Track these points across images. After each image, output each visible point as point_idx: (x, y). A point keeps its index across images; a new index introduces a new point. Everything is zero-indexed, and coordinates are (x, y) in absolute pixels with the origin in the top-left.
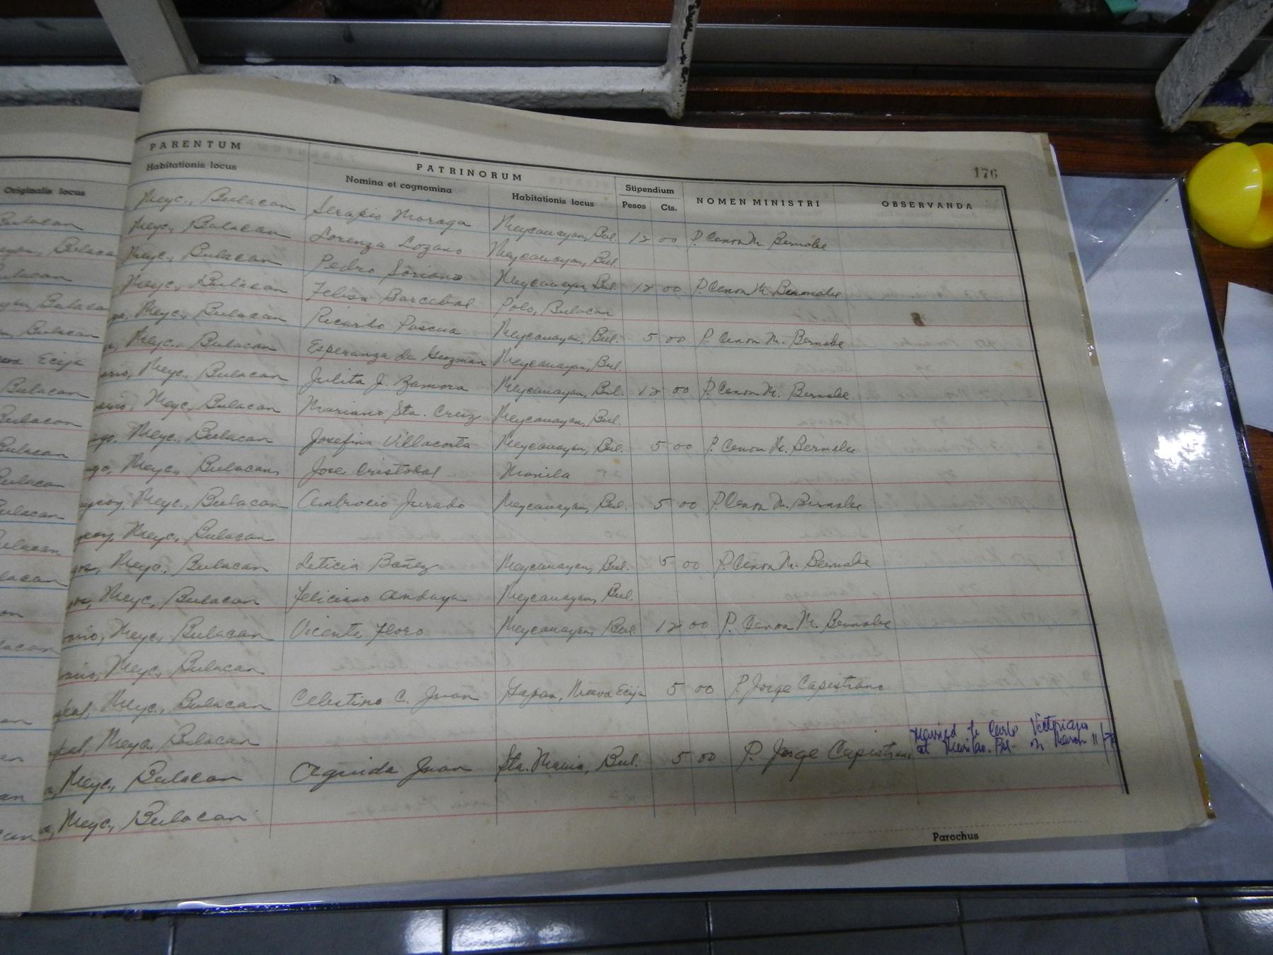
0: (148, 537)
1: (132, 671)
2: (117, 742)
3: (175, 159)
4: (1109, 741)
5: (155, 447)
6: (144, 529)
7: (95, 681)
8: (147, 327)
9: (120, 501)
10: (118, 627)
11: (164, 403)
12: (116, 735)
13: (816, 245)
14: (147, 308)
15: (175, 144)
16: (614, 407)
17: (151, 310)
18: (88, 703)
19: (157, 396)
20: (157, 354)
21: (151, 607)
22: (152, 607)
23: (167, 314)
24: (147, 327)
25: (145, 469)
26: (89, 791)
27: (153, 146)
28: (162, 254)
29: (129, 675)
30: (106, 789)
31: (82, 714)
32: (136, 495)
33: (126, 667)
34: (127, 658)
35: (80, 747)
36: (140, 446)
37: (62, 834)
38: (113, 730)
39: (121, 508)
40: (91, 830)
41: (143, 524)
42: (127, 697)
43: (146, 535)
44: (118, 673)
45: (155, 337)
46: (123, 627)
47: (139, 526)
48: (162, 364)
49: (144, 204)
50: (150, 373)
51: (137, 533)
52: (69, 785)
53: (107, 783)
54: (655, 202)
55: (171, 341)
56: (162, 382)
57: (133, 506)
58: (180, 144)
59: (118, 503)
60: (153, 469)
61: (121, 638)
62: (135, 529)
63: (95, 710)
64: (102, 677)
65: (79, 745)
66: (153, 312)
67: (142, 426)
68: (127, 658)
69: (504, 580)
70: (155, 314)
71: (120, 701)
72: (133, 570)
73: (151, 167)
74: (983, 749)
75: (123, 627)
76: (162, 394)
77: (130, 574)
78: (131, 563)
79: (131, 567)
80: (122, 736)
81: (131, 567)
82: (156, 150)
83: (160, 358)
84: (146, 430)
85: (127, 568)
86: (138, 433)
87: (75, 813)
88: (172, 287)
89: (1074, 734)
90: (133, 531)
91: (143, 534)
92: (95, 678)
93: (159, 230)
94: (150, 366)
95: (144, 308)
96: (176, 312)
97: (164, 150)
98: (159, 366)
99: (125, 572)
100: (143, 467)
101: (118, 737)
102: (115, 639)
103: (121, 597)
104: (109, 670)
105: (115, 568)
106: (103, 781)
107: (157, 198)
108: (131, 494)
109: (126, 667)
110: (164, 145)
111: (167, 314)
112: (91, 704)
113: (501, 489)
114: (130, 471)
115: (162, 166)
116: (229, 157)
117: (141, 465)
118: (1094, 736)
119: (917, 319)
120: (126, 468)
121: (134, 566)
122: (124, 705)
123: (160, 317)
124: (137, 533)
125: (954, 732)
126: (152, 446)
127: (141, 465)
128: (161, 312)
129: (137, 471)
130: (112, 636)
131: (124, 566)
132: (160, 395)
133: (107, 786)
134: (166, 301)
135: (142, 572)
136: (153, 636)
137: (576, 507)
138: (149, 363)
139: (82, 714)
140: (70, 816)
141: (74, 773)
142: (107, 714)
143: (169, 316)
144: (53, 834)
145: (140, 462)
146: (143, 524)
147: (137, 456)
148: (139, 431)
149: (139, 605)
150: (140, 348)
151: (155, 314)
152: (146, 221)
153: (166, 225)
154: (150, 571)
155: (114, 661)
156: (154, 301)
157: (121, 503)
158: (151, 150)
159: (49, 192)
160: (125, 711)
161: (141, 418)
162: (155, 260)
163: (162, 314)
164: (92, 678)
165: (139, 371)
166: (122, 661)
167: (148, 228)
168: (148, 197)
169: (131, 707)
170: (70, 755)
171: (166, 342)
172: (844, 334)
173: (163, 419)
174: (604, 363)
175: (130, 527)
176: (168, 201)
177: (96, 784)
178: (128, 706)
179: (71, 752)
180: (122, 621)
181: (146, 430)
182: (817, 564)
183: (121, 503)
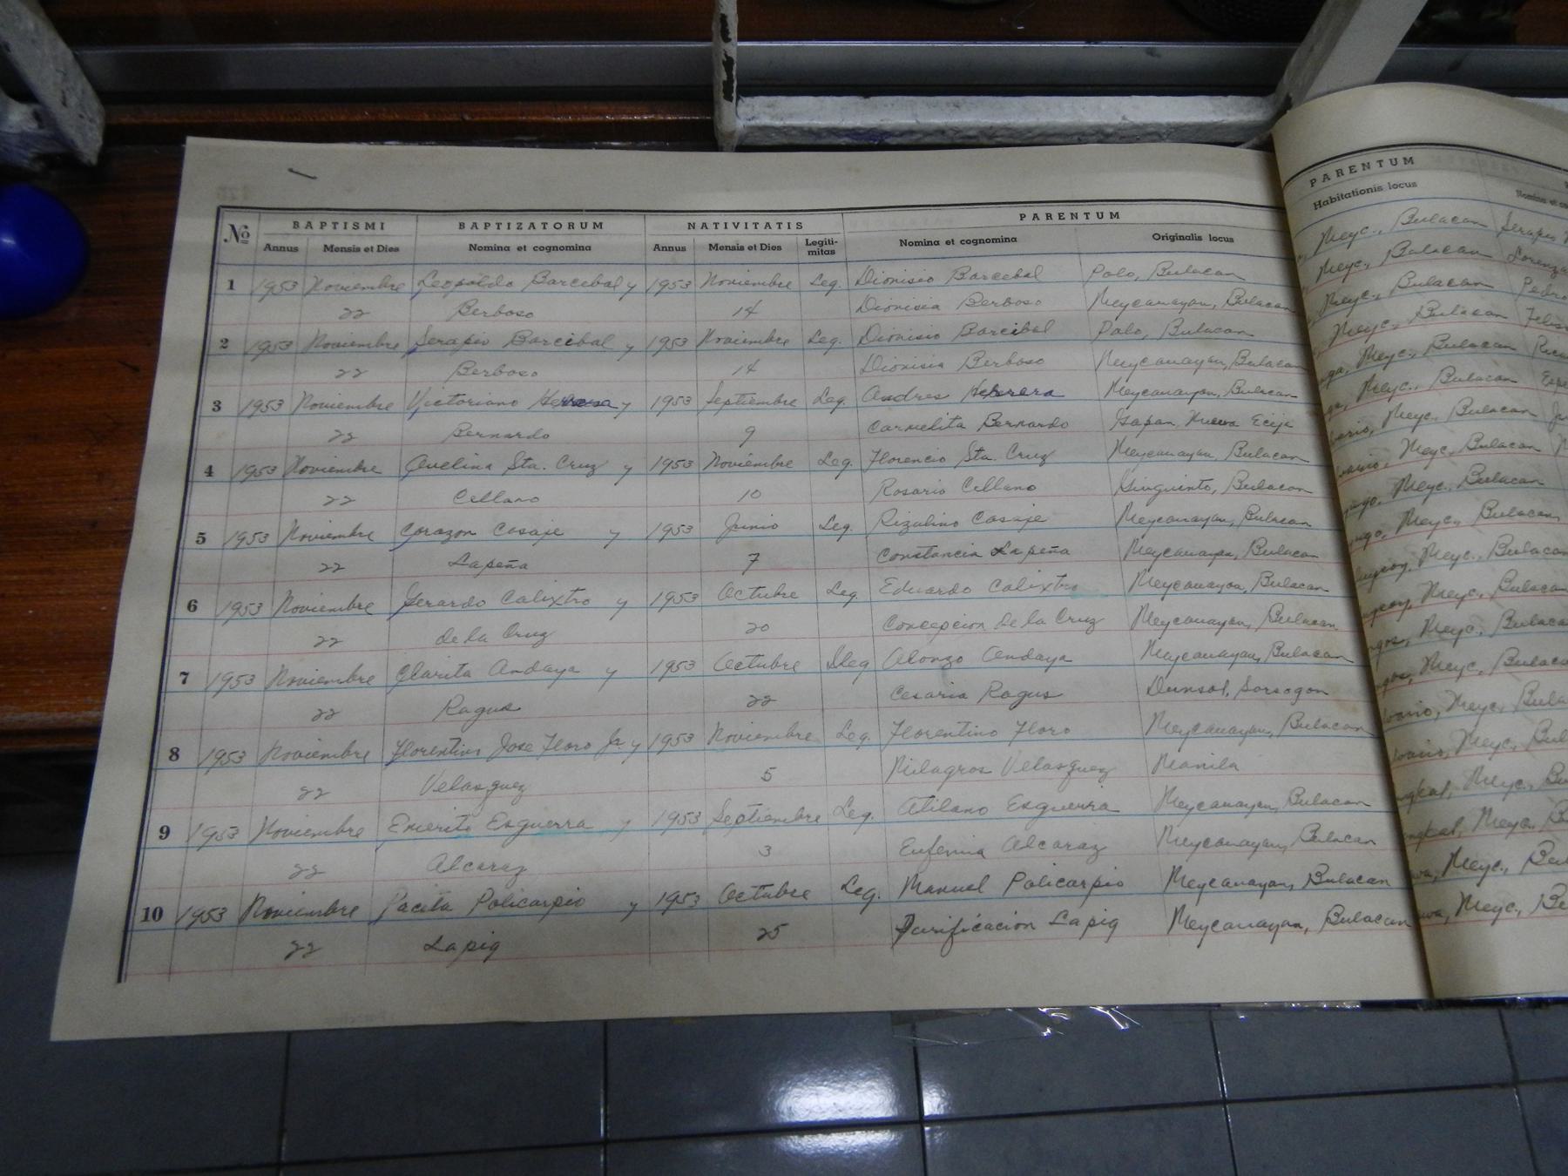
0: (1449, 597)
1: (1484, 745)
2: (1494, 822)
3: (1346, 188)
5: (1425, 500)
6: (1440, 588)
7: (1446, 758)
8: (1375, 375)
9: (1403, 563)
10: (1452, 700)
11: (1421, 450)
12: (1490, 815)
15: (1339, 173)
17: (1373, 356)
18: (1446, 783)
19: (1410, 445)
20: (1396, 401)
21: (1480, 674)
22: (1481, 673)
23: (1393, 356)
24: (1375, 375)
25: (1422, 524)
26: (1481, 874)
27: (1313, 182)
28: (1365, 294)
29: (1482, 750)
30: (1498, 871)
31: (1442, 794)
32: (1420, 553)
33: (1475, 743)
34: (1473, 731)
35: (1453, 826)
36: (1411, 501)
37: (1459, 919)
38: (1485, 808)
39: (1407, 569)
40: (1497, 913)
41: (1438, 583)
42: (1489, 772)
43: (1445, 595)
44: (1467, 749)
45: (1387, 384)
46: (1457, 699)
47: (1433, 586)
48: (1406, 410)
49: (1324, 246)
50: (1393, 423)
51: (1436, 593)
52: (1452, 868)
53: (1498, 864)
55: (1407, 383)
56: (1411, 430)
57: (1420, 565)
58: (1346, 171)
59: (1402, 566)
60: (1430, 523)
61: (1459, 711)
62: (1430, 590)
63: (1457, 789)
64: (1452, 754)
65: (1451, 825)
66: (1376, 357)
67: (1404, 480)
68: (1473, 731)
70: (1379, 359)
71: (1481, 778)
72: (1445, 635)
73: (1318, 205)
75: (1457, 699)
76: (1414, 443)
77: (1444, 640)
78: (1441, 628)
79: (1442, 632)
80: (1497, 813)
81: (1442, 632)
82: (1319, 184)
83: (1401, 405)
84: (1408, 486)
85: (1438, 634)
86: (1402, 488)
87: (1470, 896)
88: (1388, 326)
90: (1430, 593)
91: (1442, 593)
92: (1444, 755)
93: (1353, 269)
94: (1393, 415)
95: (1364, 355)
96: (1403, 351)
97: (1328, 183)
98: (1403, 413)
99: (1438, 639)
100: (1418, 522)
101: (1493, 816)
102: (1452, 713)
103: (1443, 666)
104: (1458, 746)
105: (1424, 636)
106: (1492, 863)
107: (1337, 237)
108: (1413, 553)
109: (1475, 743)
110: (1326, 177)
111: (1393, 356)
112: (1449, 783)
114: (1405, 529)
115: (1332, 200)
117: (1415, 521)
120: (1399, 528)
121: (1445, 631)
122: (1487, 782)
123: (1386, 360)
124: (1436, 593)
126: (1422, 499)
127: (1415, 521)
128: (1386, 355)
129: (1412, 528)
130: (1449, 709)
131: (1434, 633)
132: (1414, 443)
133: (1500, 867)
134: (1385, 342)
135: (1455, 637)
136: (1493, 705)
138: (1390, 413)
139: (1442, 794)
141: (1454, 856)
142: (1471, 793)
143: (1396, 358)
144: (1448, 918)
145: (1413, 518)
146: (1438, 583)
147: (1408, 512)
148: (1403, 485)
149: (1465, 673)
150: (1376, 398)
151: (1379, 359)
152: (1335, 263)
153: (1359, 262)
154: (1464, 634)
155: (1461, 736)
156: (1374, 345)
157: (1406, 564)
158: (1312, 186)
159: (1200, 239)
160: (1491, 789)
161: (1401, 472)
162: (1359, 302)
163: (1387, 357)
164: (1440, 756)
165: (1381, 424)
166: (1469, 735)
167: (1339, 270)
168: (1327, 237)
169: (1497, 783)
170: (1442, 837)
171: (1402, 385)
173: (1425, 468)
175: (1426, 588)
176: (1353, 235)
177: (1485, 866)
178: (1492, 783)
179: (1442, 833)
180: (1454, 693)
181: (1410, 484)
183: (1406, 564)
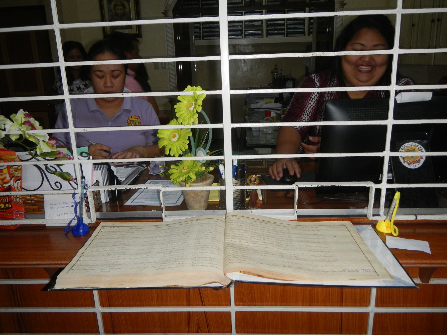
4: (374, 272)
13: (318, 231)
14: (231, 228)
16: (292, 243)
54: (295, 227)
69: (280, 254)
74: (354, 272)
89: (369, 271)
113: (278, 248)
116: (240, 218)
118: (372, 271)
119: (335, 237)
125: (349, 270)
137: (289, 250)
140: (230, 262)
172: (324, 238)
174: (290, 239)
182: (325, 256)
